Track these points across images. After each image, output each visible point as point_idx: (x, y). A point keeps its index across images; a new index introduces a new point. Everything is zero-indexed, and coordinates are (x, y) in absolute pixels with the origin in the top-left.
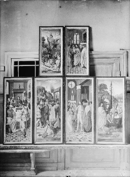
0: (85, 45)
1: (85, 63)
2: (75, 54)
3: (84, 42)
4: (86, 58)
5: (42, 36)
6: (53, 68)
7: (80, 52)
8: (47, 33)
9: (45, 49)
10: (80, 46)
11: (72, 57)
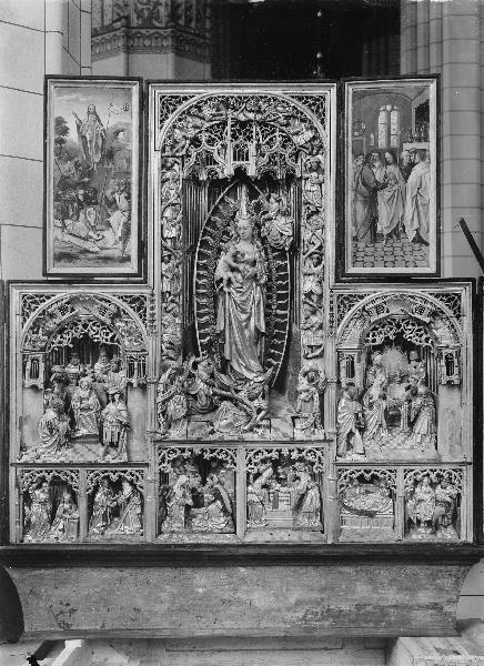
0: (423, 154)
1: (423, 222)
2: (384, 186)
3: (419, 140)
4: (426, 205)
5: (57, 111)
6: (100, 244)
7: (401, 183)
8: (76, 100)
9: (69, 165)
10: (404, 154)
11: (371, 202)
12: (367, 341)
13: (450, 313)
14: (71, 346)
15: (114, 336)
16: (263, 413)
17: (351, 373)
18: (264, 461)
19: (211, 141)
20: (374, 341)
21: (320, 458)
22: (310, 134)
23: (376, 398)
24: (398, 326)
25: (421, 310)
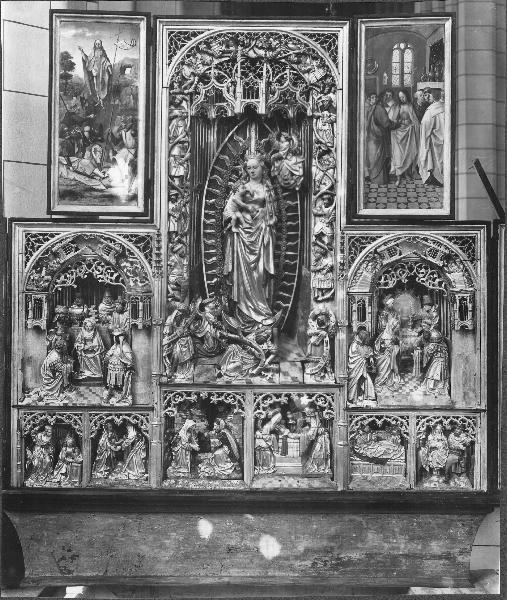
0: (438, 94)
1: (438, 163)
2: (397, 126)
3: (434, 79)
4: (440, 146)
5: (62, 46)
6: (105, 182)
7: (415, 122)
8: (83, 36)
9: (75, 100)
10: (418, 93)
11: (384, 143)
13: (463, 256)
14: (75, 286)
15: (119, 276)
16: (272, 356)
18: (272, 406)
19: (220, 79)
20: (386, 284)
22: (319, 73)
23: (387, 342)
24: (411, 269)
25: (434, 253)
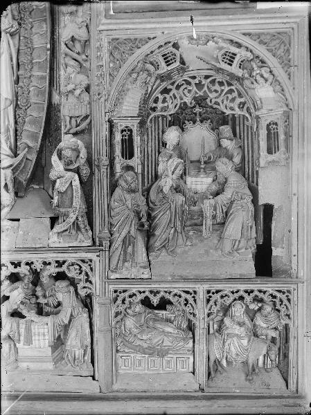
12: (154, 109)
13: (272, 62)
17: (128, 152)
21: (87, 274)
24: (199, 86)
